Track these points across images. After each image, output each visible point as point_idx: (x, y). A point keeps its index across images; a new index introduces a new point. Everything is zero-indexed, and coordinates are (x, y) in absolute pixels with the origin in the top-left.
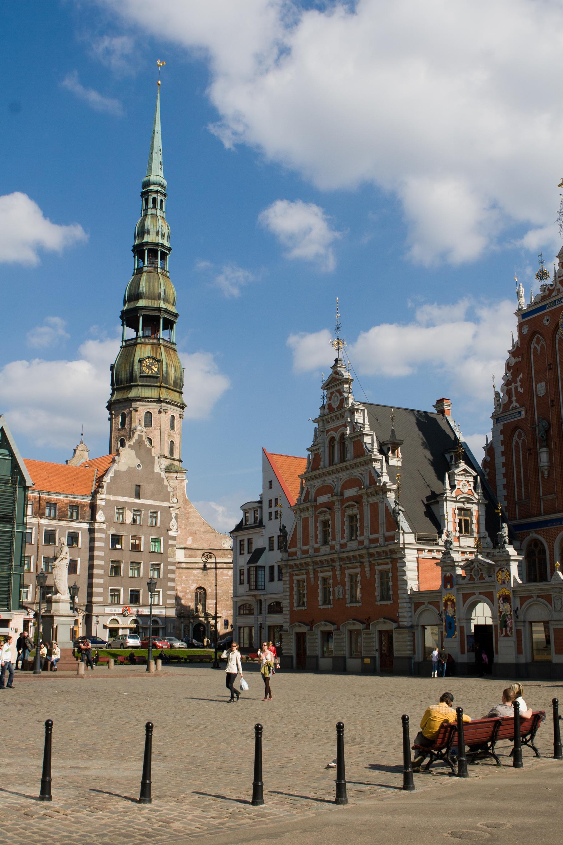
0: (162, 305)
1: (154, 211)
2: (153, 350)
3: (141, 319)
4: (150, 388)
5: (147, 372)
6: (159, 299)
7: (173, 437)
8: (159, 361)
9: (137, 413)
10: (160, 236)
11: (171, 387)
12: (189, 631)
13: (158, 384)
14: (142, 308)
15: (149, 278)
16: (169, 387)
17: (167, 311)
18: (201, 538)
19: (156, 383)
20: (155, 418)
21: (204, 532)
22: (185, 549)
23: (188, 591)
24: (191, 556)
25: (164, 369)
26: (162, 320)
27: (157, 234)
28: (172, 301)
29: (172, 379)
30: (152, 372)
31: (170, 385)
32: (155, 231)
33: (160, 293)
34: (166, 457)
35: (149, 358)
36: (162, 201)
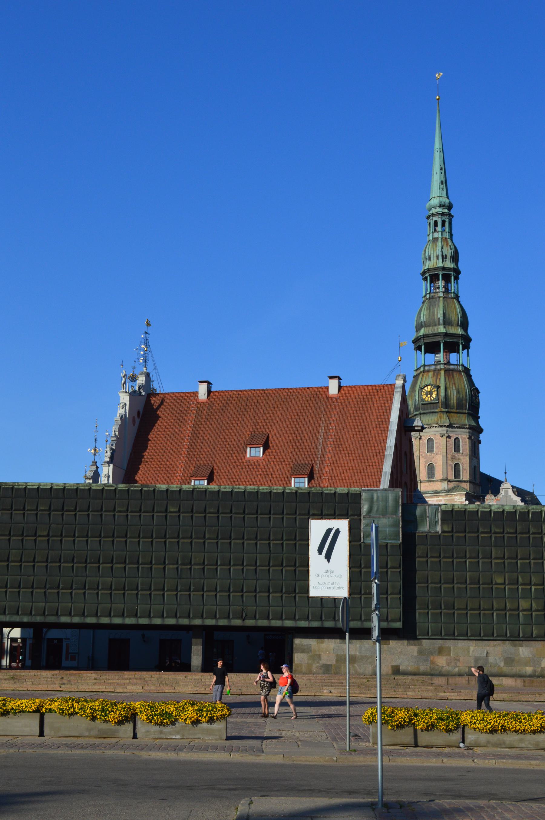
0: (442, 330)
4: (431, 415)
5: (427, 399)
6: (439, 324)
7: (459, 459)
9: (421, 441)
10: (440, 259)
11: (454, 410)
14: (424, 336)
15: (430, 305)
16: (452, 410)
19: (437, 408)
20: (436, 443)
26: (442, 345)
27: (438, 258)
29: (454, 400)
31: (453, 409)
32: (435, 255)
33: (439, 319)
36: (443, 223)
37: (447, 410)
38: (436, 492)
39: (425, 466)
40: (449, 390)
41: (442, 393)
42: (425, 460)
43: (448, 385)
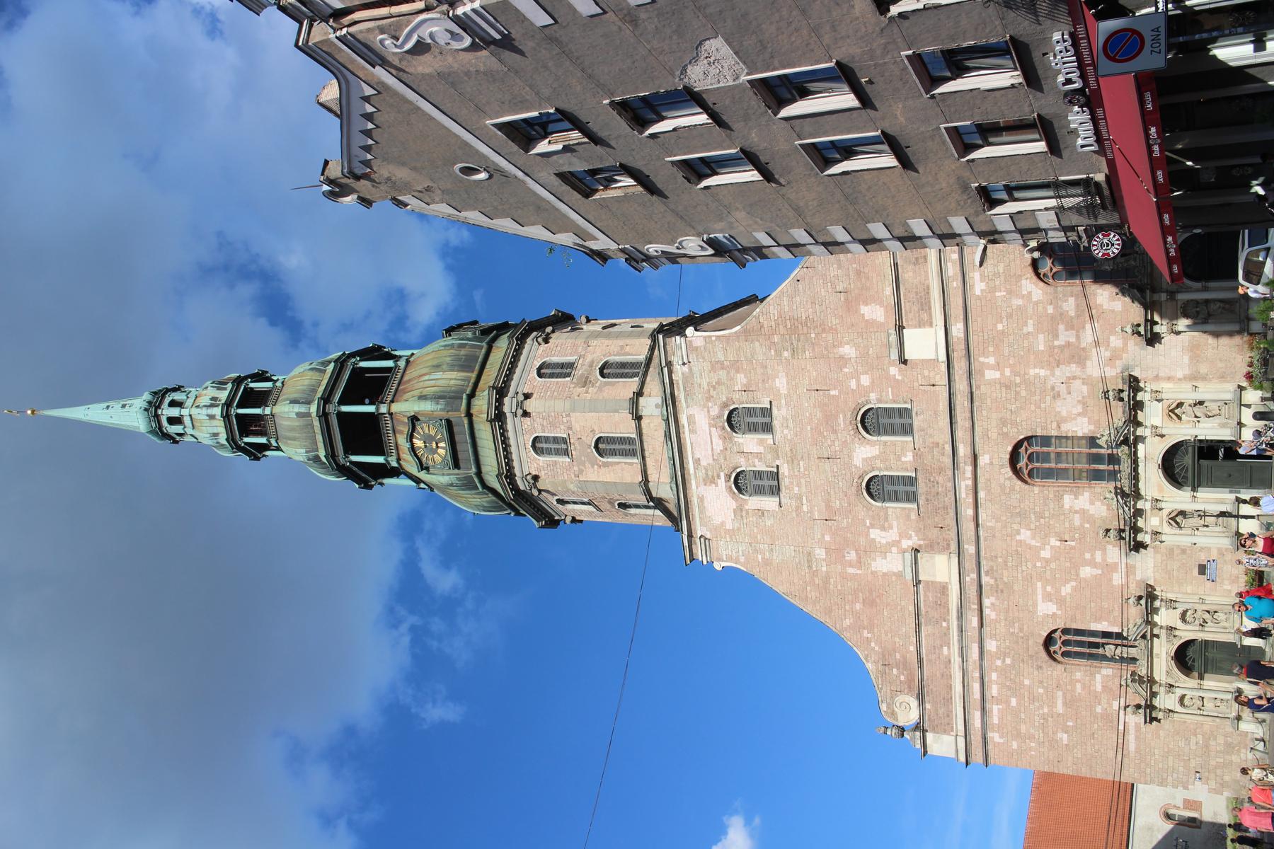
0: (313, 408)
1: (187, 420)
2: (401, 432)
3: (355, 458)
6: (308, 415)
7: (591, 365)
8: (414, 419)
9: (542, 474)
11: (474, 375)
12: (1207, 302)
13: (466, 421)
14: (332, 454)
17: (326, 399)
18: (858, 273)
21: (840, 267)
22: (900, 328)
23: (1050, 310)
24: (925, 306)
25: (427, 407)
26: (345, 409)
28: (316, 376)
30: (441, 440)
32: (208, 423)
33: (299, 415)
34: (639, 394)
35: (413, 449)
36: (173, 404)
37: (464, 396)
38: (668, 435)
39: (605, 465)
40: (425, 392)
41: (427, 407)
42: (588, 465)
43: (416, 393)
